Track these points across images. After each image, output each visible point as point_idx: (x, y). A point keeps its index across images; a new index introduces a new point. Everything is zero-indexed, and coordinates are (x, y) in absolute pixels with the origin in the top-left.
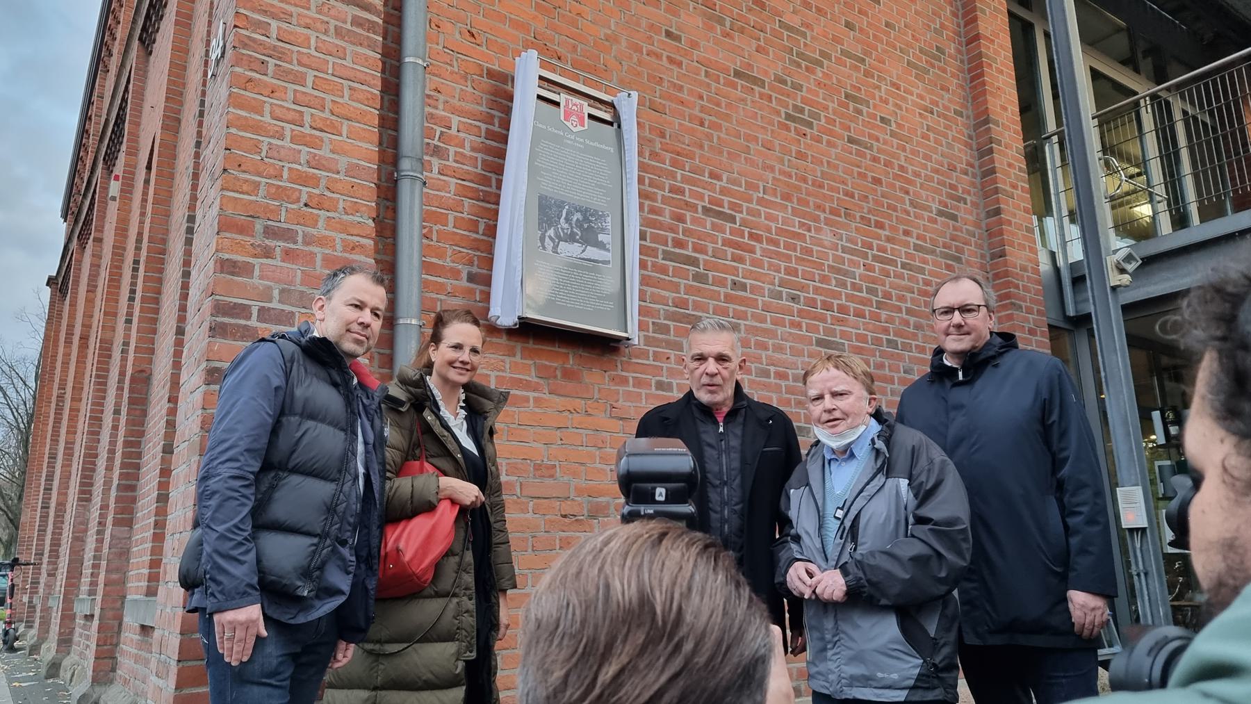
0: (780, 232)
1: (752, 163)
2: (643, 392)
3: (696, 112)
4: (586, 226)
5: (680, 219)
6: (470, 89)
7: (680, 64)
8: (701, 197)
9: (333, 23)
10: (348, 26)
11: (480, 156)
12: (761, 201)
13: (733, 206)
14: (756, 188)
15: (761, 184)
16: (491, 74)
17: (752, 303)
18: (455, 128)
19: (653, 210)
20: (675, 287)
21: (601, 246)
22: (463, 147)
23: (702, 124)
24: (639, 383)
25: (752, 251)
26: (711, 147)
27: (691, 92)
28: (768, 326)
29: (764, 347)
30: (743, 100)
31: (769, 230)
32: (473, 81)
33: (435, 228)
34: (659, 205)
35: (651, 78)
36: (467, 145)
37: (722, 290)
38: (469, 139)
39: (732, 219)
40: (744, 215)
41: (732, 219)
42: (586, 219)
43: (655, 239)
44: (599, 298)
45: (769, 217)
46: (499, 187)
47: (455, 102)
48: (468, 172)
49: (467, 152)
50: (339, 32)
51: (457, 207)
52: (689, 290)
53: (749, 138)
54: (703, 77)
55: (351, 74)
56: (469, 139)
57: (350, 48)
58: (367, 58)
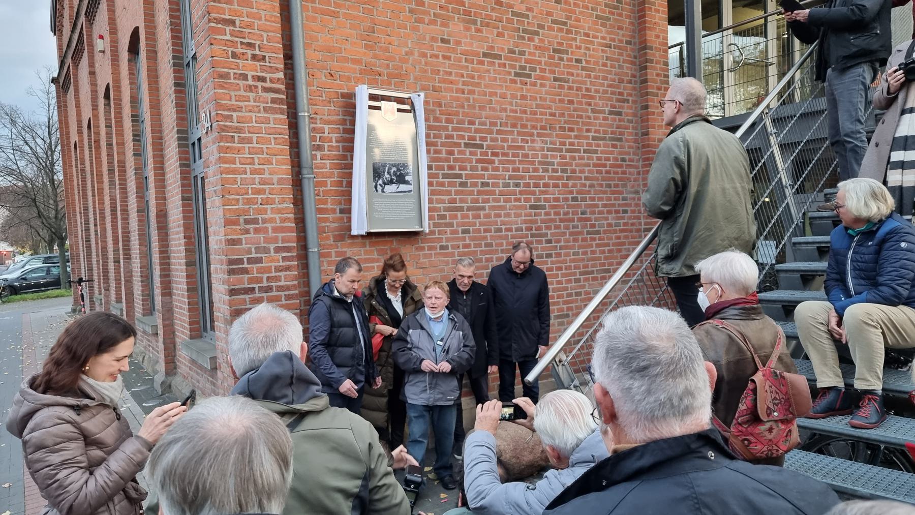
0: (510, 147)
1: (493, 109)
2: (433, 252)
3: (460, 86)
5: (451, 153)
6: (333, 108)
7: (449, 58)
8: (463, 137)
9: (262, 105)
10: (269, 105)
11: (340, 144)
12: (498, 132)
13: (482, 139)
14: (495, 124)
15: (499, 121)
16: (343, 96)
17: (493, 193)
18: (326, 131)
19: (436, 152)
20: (449, 193)
21: (407, 183)
22: (331, 142)
23: (463, 93)
24: (430, 248)
25: (493, 162)
26: (469, 106)
27: (457, 74)
28: (502, 203)
29: (499, 216)
30: (488, 71)
31: (503, 148)
33: (321, 189)
34: (439, 148)
35: (433, 72)
36: (334, 140)
37: (475, 189)
38: (334, 136)
39: (481, 146)
40: (489, 142)
41: (481, 146)
42: (398, 170)
43: (438, 168)
45: (503, 140)
46: (352, 159)
47: (325, 117)
48: (335, 155)
49: (334, 144)
50: (266, 110)
51: (331, 175)
52: (457, 193)
53: (491, 94)
54: (464, 63)
55: (273, 131)
56: (334, 136)
57: (272, 116)
58: (280, 119)
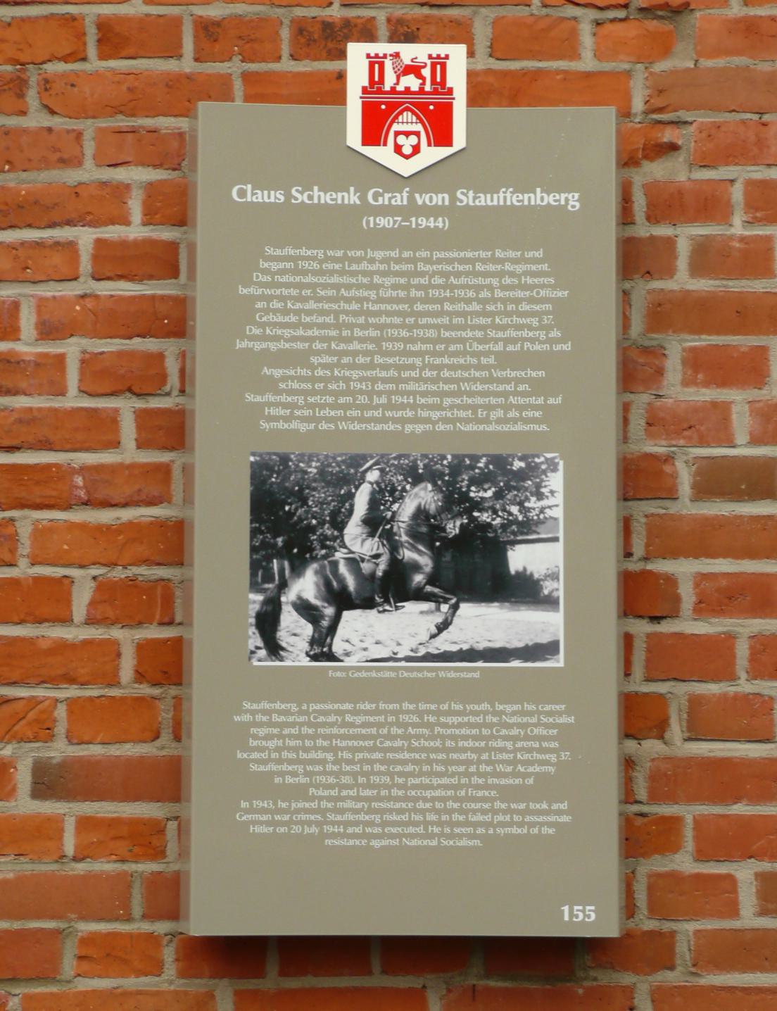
4: (453, 528)
21: (522, 591)
32: (46, 84)
42: (455, 501)
44: (508, 794)
